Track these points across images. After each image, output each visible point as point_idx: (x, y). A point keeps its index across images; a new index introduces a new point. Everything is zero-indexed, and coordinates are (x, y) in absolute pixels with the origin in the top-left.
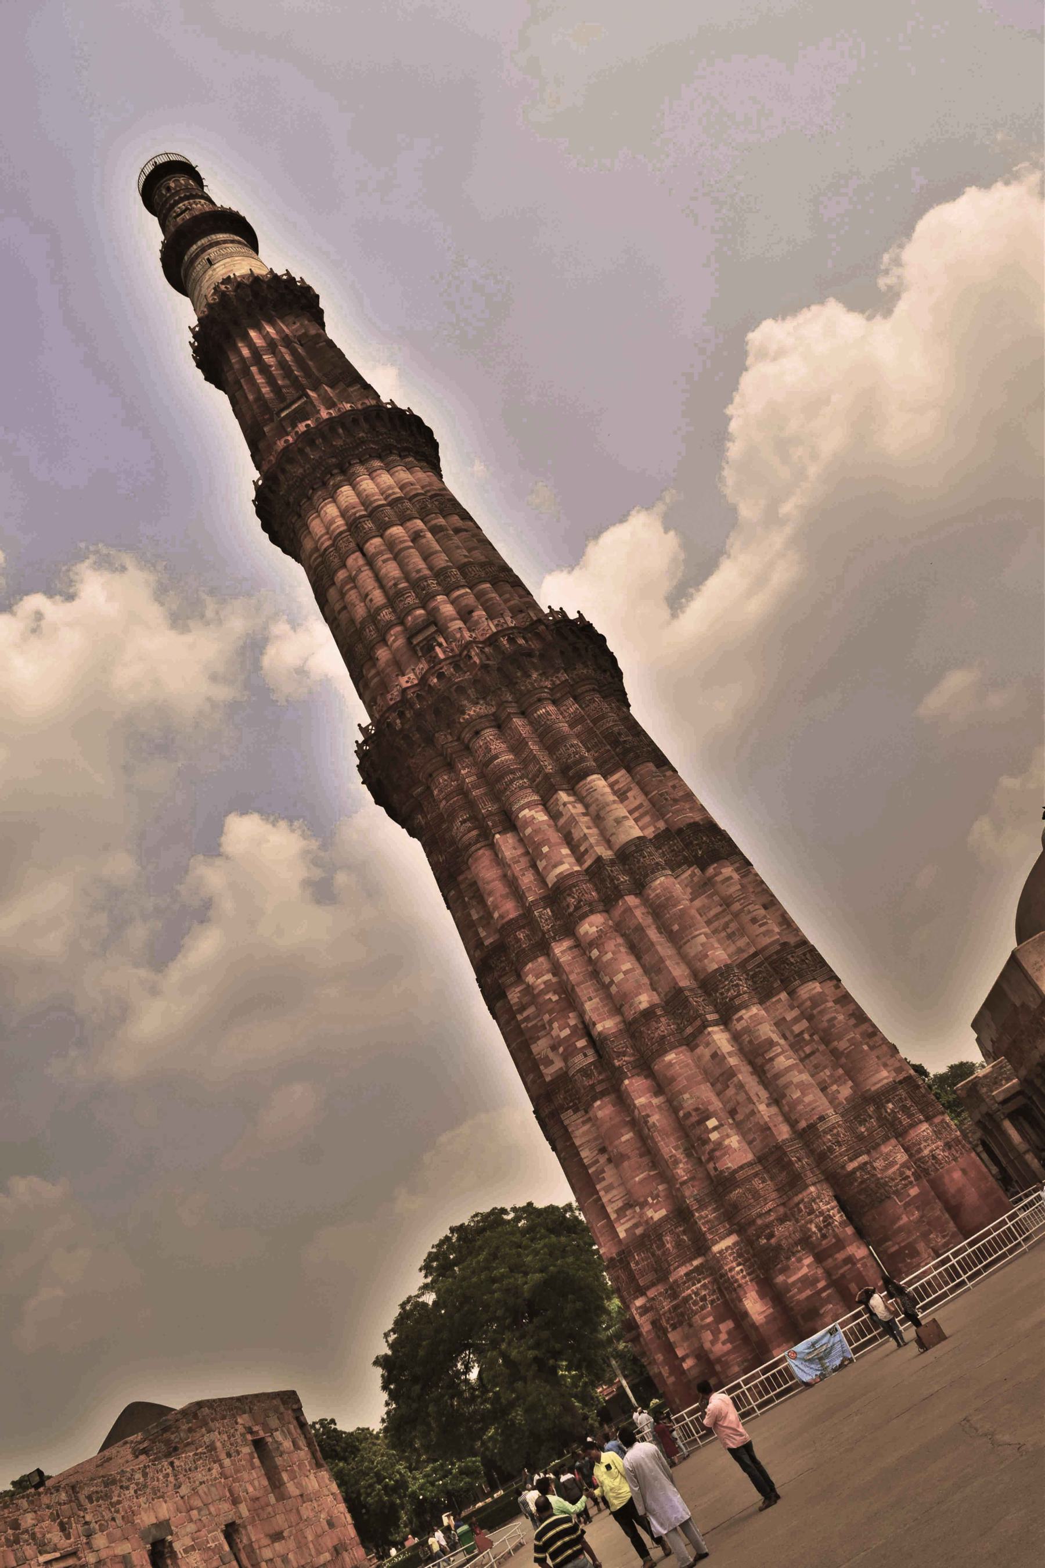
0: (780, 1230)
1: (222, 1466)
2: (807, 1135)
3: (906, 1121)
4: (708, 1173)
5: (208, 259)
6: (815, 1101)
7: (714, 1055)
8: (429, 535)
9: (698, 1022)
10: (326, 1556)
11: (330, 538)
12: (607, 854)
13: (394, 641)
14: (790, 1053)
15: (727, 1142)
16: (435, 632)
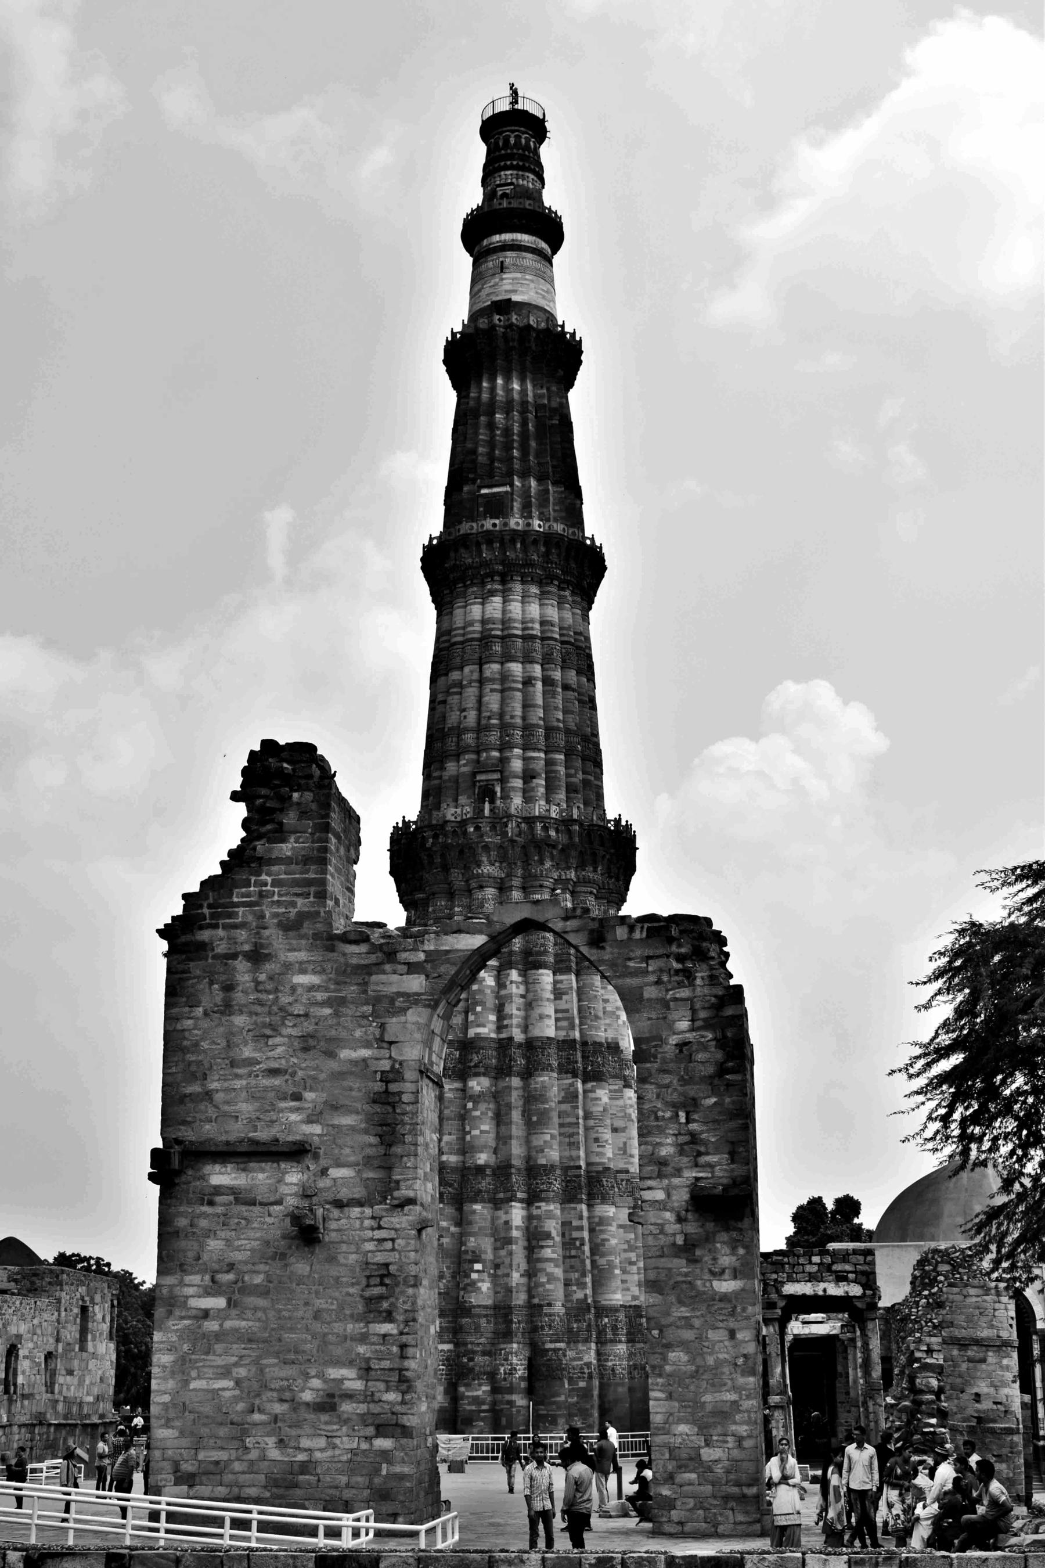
0: (479, 1359)
1: (59, 1315)
2: (535, 1309)
3: (610, 1336)
4: (458, 1297)
5: (502, 262)
6: (553, 1291)
7: (507, 1223)
8: (539, 685)
9: (509, 1194)
10: (90, 1399)
11: (463, 635)
12: (518, 1036)
13: (464, 765)
14: (560, 1250)
15: (480, 1284)
16: (497, 780)
